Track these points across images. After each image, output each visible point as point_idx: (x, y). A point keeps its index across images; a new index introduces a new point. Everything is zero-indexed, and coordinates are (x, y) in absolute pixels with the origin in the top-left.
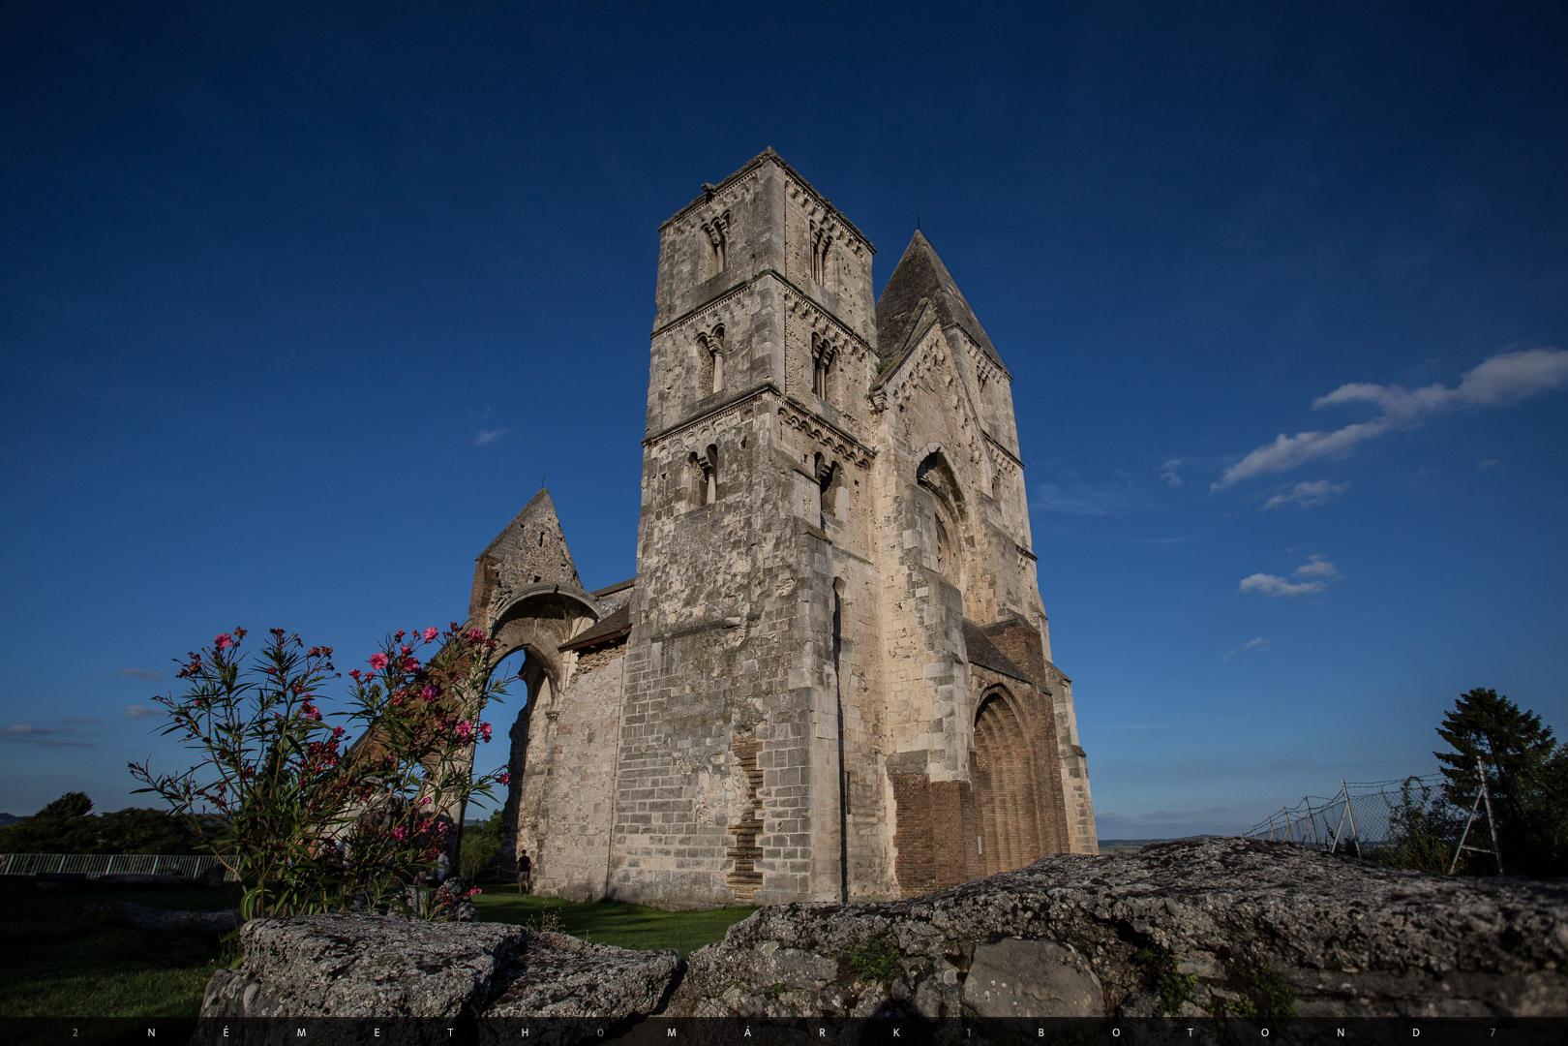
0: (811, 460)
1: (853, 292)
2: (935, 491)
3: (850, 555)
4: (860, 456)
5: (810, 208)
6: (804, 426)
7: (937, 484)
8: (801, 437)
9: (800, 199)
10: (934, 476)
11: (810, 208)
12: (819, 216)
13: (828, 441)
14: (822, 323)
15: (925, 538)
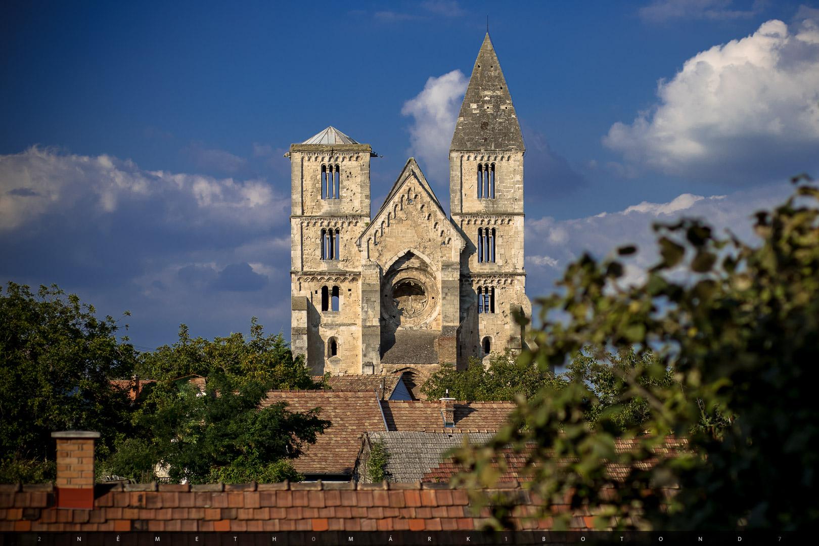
0: (320, 292)
1: (353, 187)
2: (416, 269)
3: (340, 325)
4: (351, 278)
5: (320, 159)
6: (313, 279)
7: (417, 265)
8: (312, 284)
9: (313, 158)
10: (414, 263)
11: (320, 159)
12: (327, 159)
13: (329, 279)
14: (326, 223)
15: (370, 312)
